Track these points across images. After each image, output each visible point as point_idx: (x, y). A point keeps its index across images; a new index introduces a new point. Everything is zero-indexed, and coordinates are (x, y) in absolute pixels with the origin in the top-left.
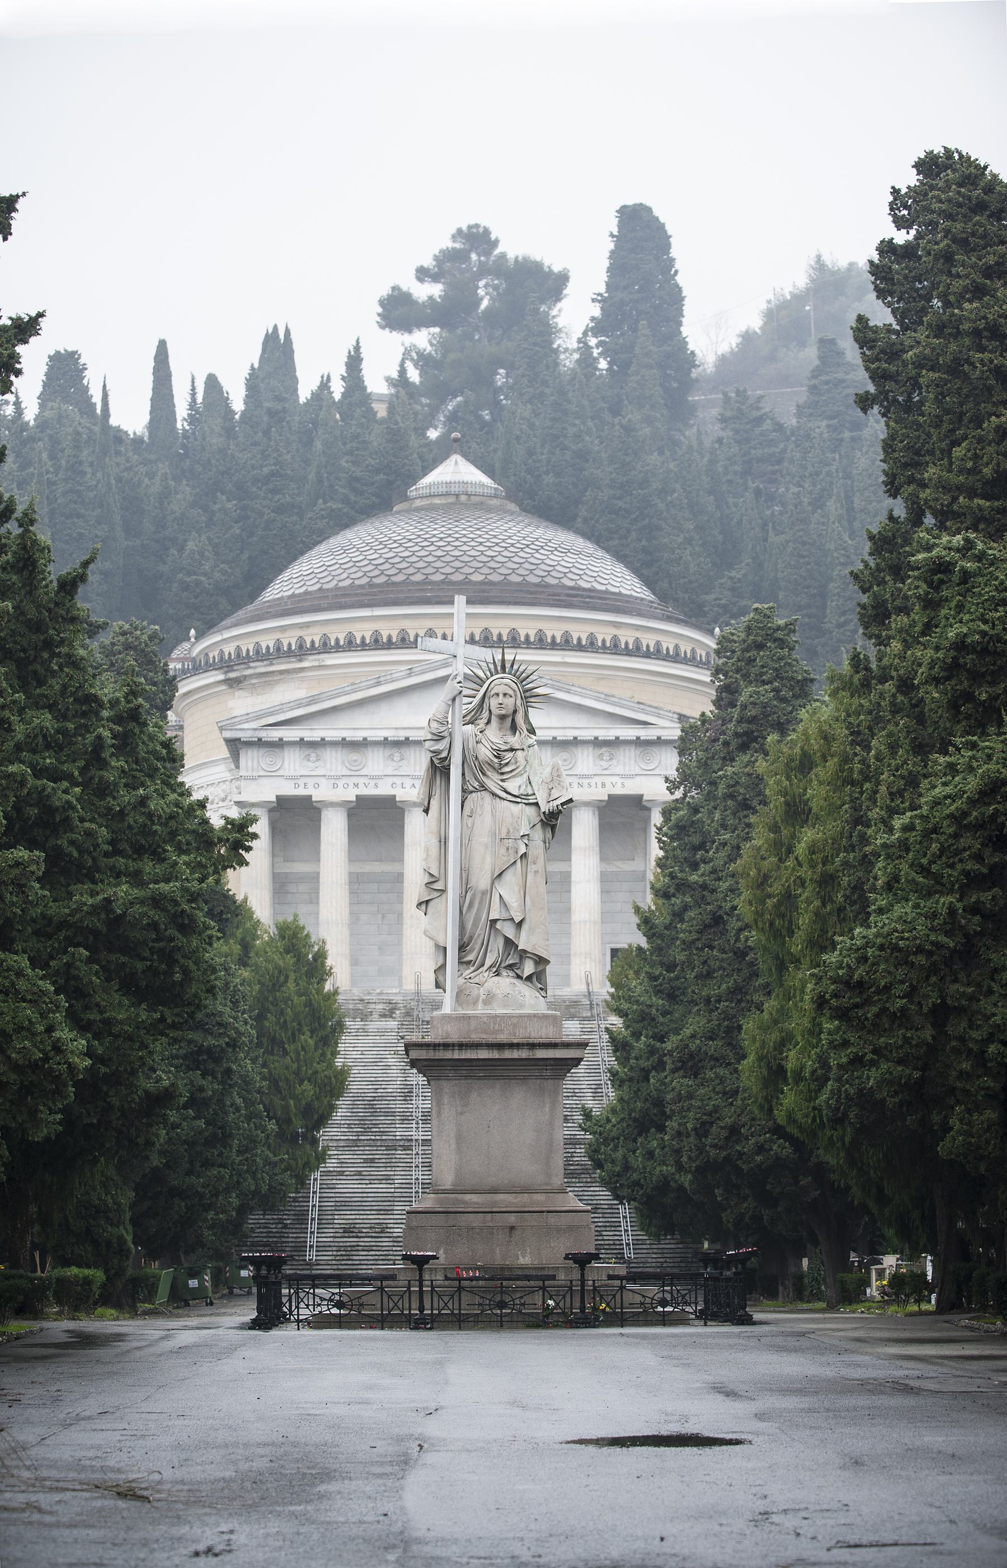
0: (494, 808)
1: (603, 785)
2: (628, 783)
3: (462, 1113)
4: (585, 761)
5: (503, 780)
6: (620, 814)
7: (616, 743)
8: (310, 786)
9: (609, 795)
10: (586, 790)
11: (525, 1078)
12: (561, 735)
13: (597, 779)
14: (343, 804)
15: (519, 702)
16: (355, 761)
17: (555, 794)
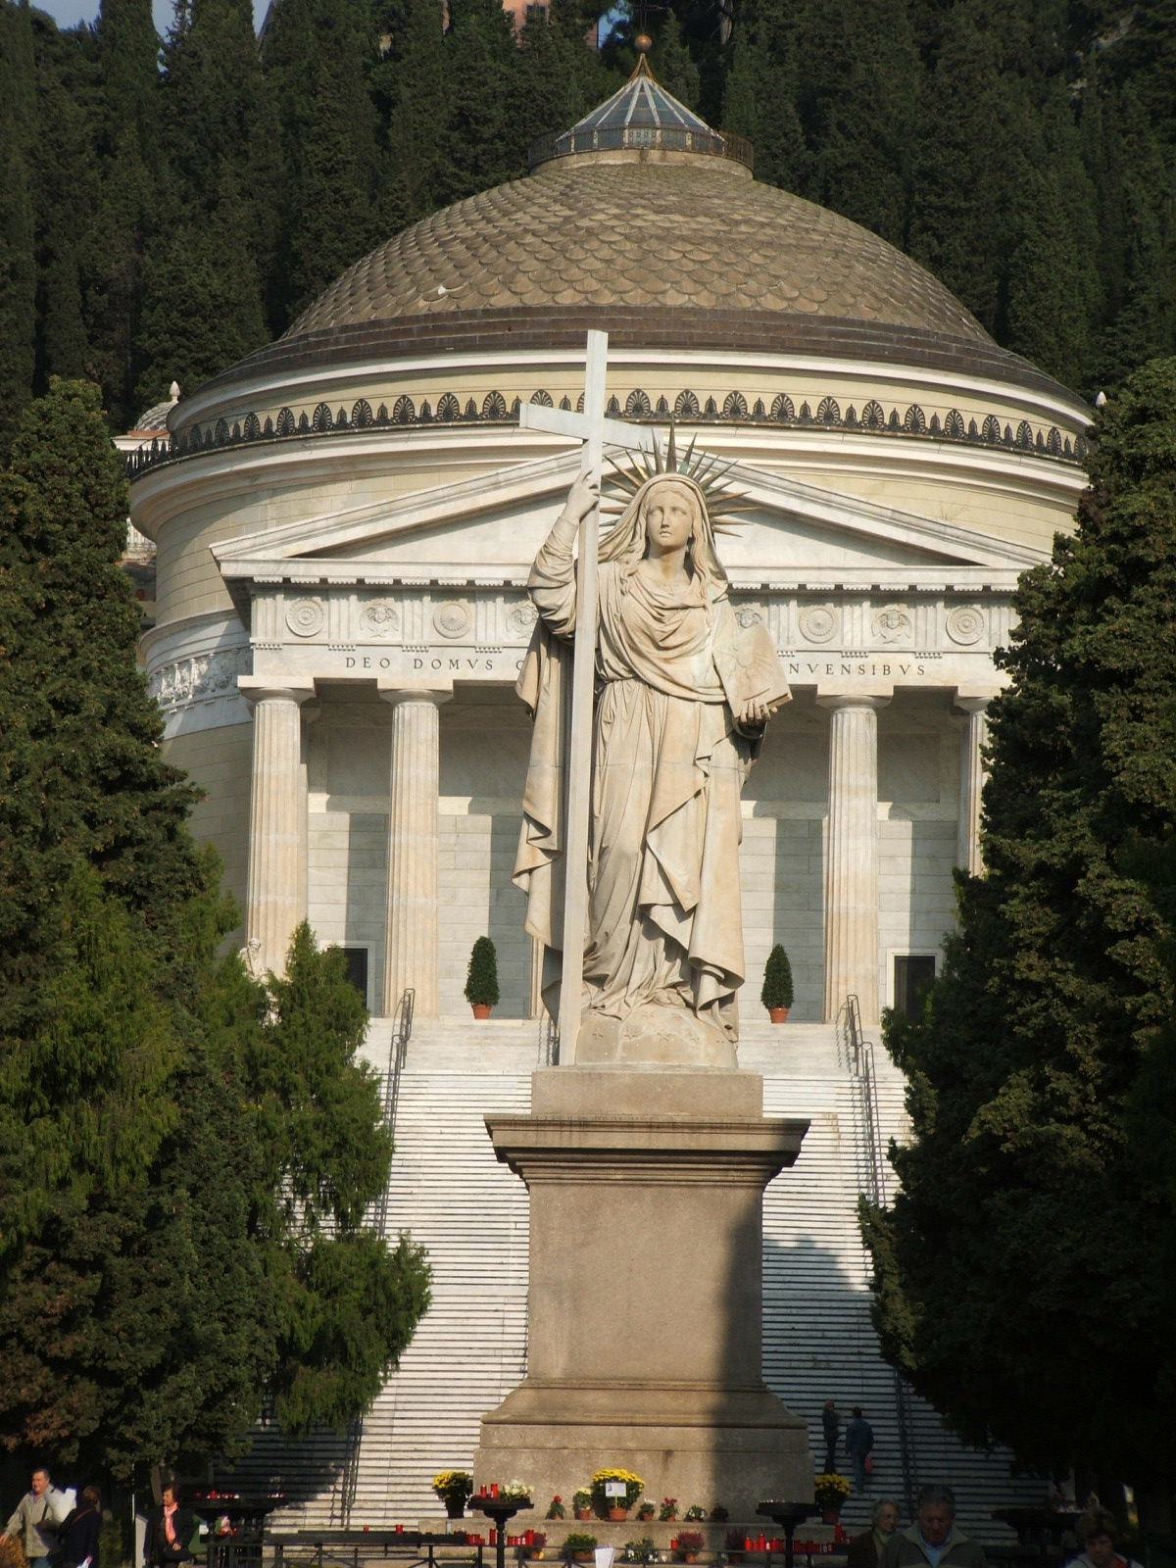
0: (650, 708)
1: (887, 669)
3: (583, 1245)
5: (667, 660)
6: (917, 722)
7: (914, 597)
8: (374, 663)
9: (895, 688)
10: (855, 676)
11: (694, 1185)
12: (815, 581)
13: (873, 658)
14: (436, 696)
15: (698, 524)
17: (759, 686)
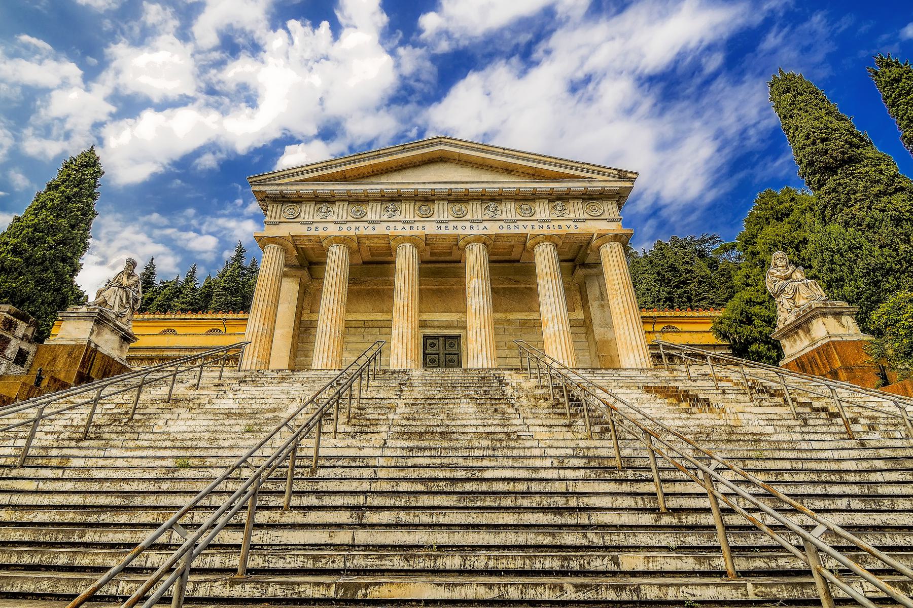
1: (560, 227)
2: (579, 225)
4: (542, 210)
13: (553, 223)
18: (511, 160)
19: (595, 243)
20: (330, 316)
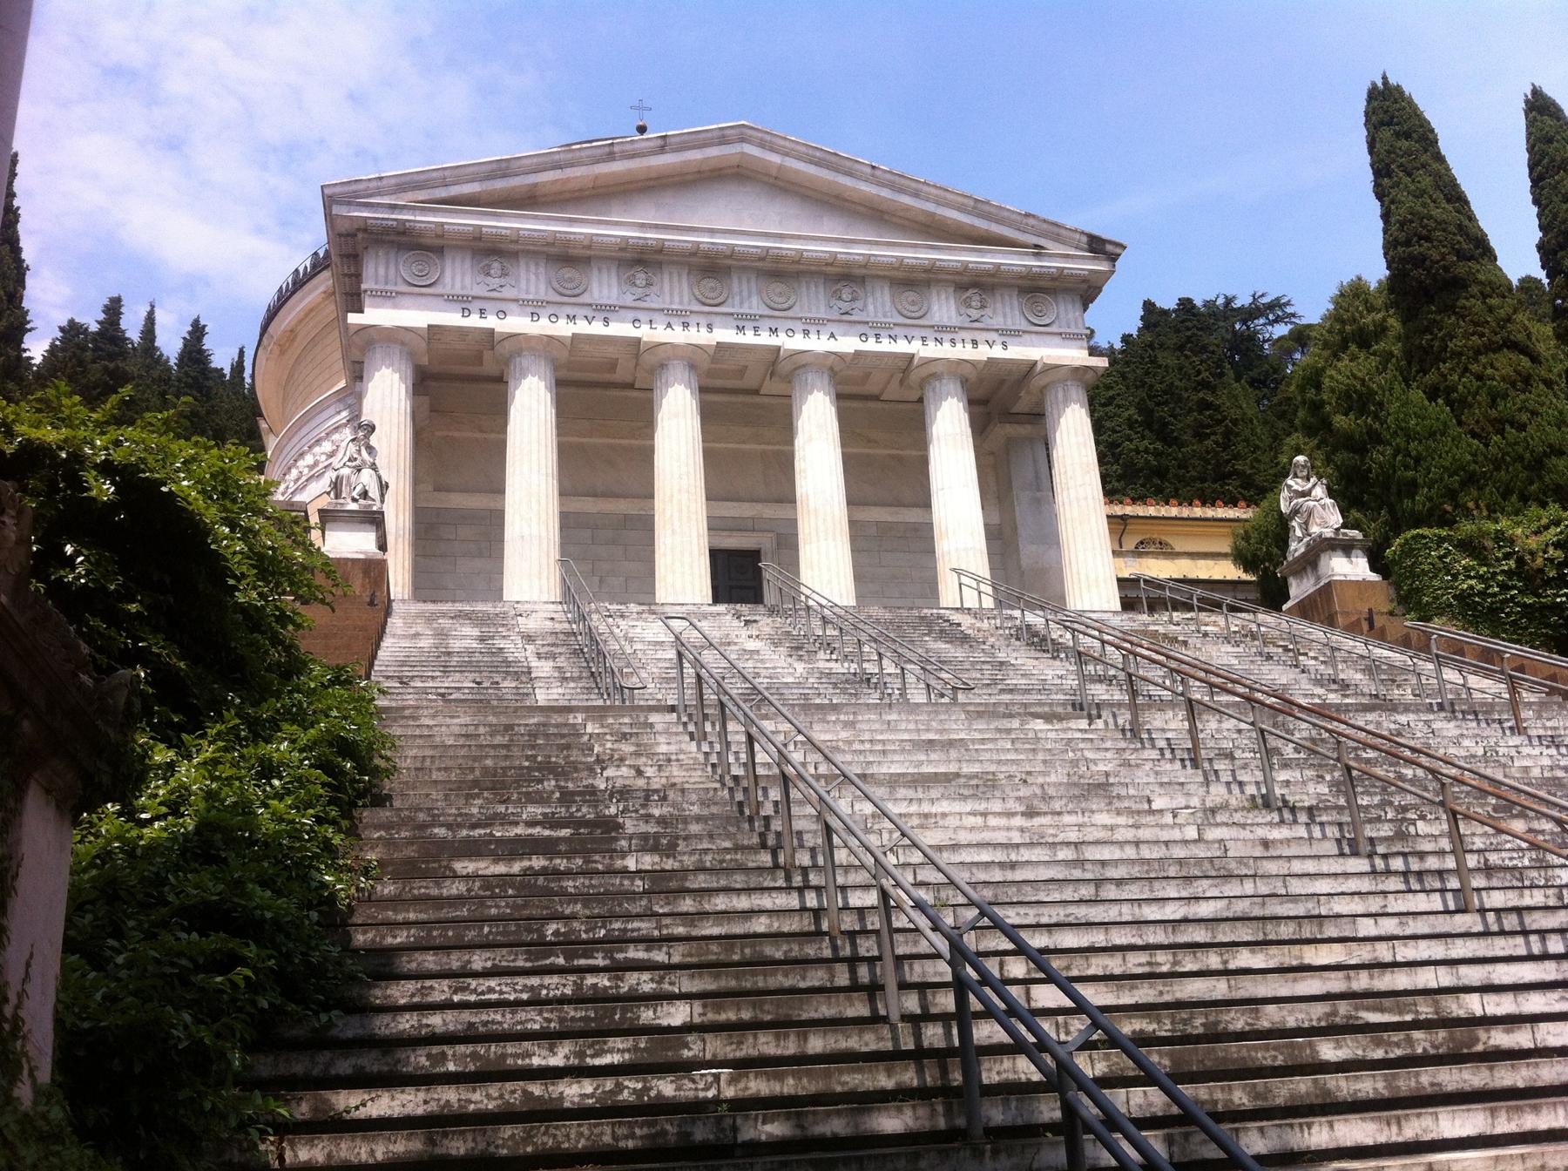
16: (571, 280)
18: (885, 193)
19: (1037, 382)
20: (535, 507)
